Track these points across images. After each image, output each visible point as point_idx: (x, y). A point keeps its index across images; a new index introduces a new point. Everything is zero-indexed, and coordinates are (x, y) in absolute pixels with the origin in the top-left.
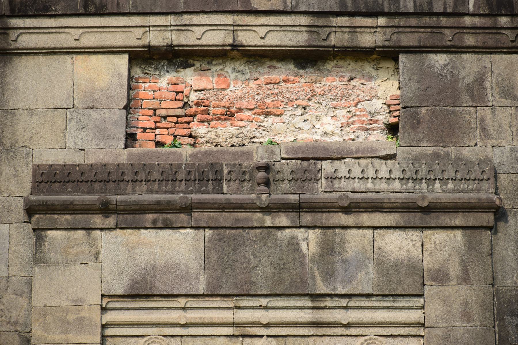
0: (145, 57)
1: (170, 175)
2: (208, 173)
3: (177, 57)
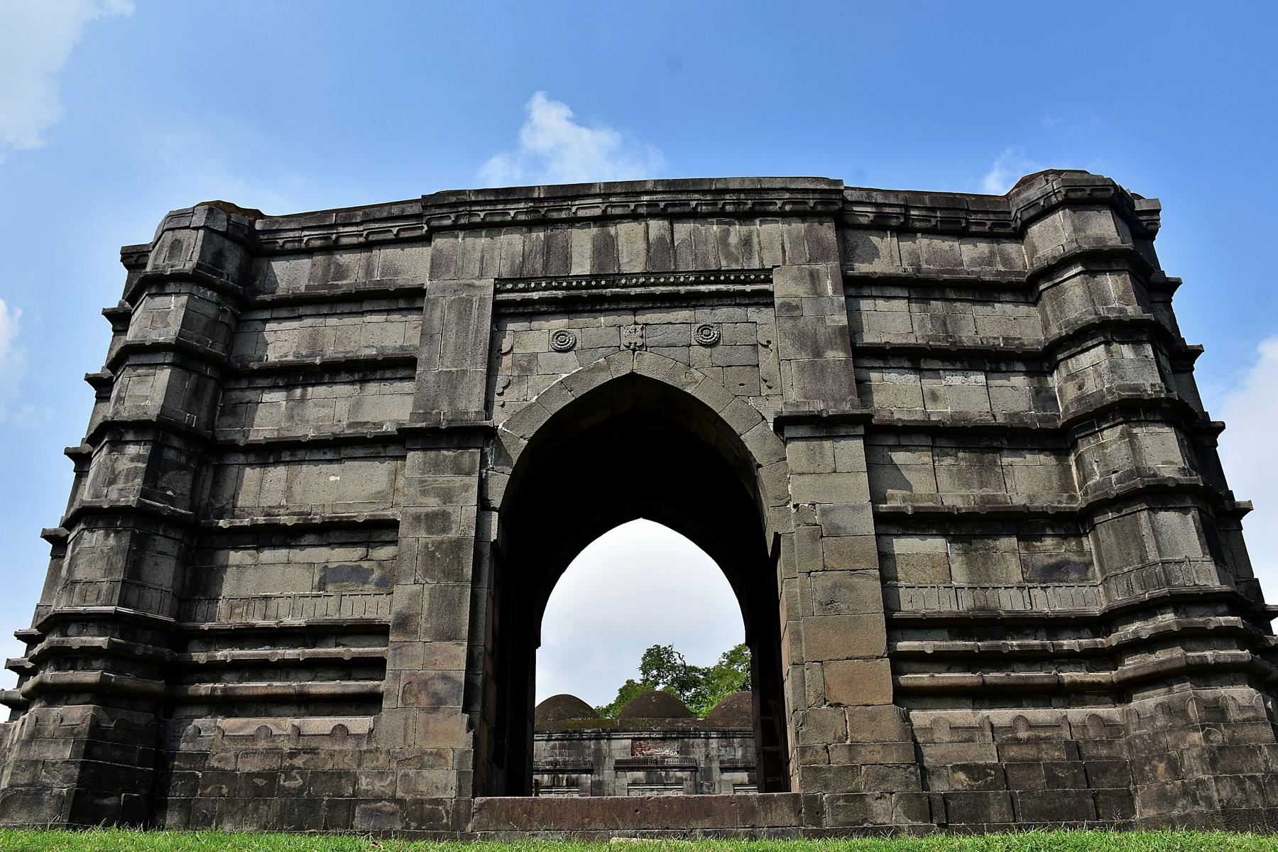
1: (639, 761)
2: (645, 761)
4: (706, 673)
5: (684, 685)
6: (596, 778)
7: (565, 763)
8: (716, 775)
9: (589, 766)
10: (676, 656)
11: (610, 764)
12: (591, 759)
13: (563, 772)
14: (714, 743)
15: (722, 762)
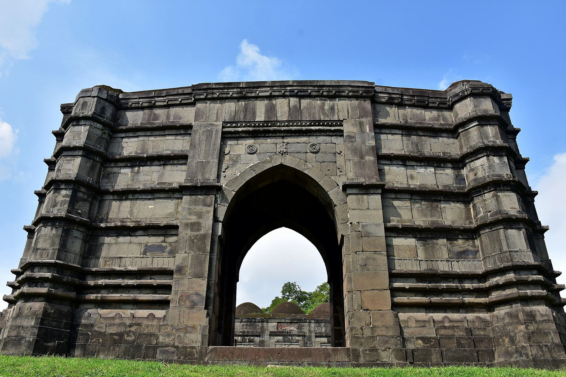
0: (278, 322)
1: (280, 332)
2: (283, 332)
3: (281, 322)
4: (310, 294)
5: (300, 300)
6: (261, 339)
7: (248, 332)
8: (313, 339)
9: (258, 334)
10: (297, 287)
11: (267, 333)
12: (259, 331)
13: (247, 336)
14: (313, 325)
15: (316, 333)
